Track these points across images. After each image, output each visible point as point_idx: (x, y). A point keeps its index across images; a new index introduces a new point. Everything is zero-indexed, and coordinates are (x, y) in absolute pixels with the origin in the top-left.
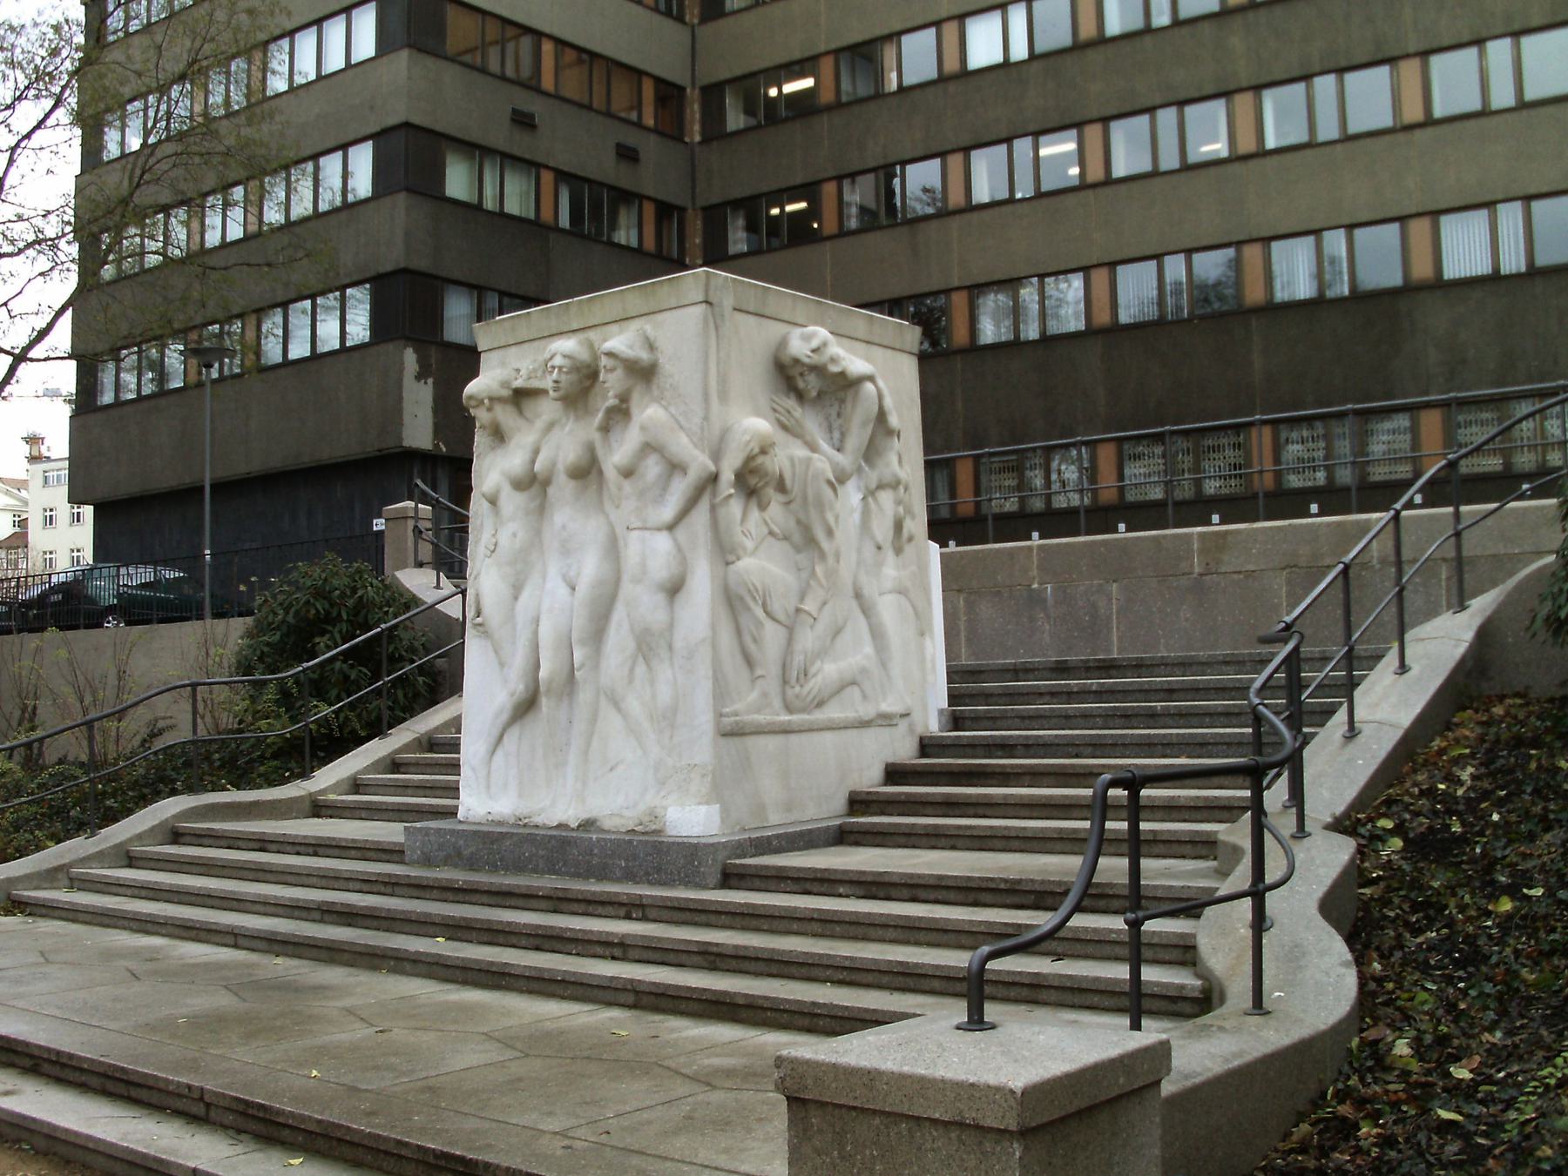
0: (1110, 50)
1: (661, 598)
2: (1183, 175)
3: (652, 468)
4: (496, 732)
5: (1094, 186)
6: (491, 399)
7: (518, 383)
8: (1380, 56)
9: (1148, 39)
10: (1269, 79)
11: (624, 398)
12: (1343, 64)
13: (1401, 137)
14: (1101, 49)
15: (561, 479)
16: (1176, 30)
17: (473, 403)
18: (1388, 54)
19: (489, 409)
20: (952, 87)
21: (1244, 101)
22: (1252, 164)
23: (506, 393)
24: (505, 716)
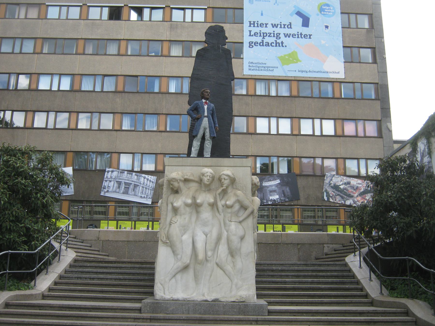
1: (240, 240)
3: (237, 207)
4: (174, 274)
5: (72, 129)
7: (186, 177)
9: (94, 93)
11: (227, 187)
12: (146, 112)
13: (159, 133)
14: (80, 93)
15: (206, 205)
16: (102, 93)
17: (173, 180)
18: (158, 113)
19: (178, 183)
20: (33, 93)
22: (118, 132)
23: (183, 179)
24: (179, 269)
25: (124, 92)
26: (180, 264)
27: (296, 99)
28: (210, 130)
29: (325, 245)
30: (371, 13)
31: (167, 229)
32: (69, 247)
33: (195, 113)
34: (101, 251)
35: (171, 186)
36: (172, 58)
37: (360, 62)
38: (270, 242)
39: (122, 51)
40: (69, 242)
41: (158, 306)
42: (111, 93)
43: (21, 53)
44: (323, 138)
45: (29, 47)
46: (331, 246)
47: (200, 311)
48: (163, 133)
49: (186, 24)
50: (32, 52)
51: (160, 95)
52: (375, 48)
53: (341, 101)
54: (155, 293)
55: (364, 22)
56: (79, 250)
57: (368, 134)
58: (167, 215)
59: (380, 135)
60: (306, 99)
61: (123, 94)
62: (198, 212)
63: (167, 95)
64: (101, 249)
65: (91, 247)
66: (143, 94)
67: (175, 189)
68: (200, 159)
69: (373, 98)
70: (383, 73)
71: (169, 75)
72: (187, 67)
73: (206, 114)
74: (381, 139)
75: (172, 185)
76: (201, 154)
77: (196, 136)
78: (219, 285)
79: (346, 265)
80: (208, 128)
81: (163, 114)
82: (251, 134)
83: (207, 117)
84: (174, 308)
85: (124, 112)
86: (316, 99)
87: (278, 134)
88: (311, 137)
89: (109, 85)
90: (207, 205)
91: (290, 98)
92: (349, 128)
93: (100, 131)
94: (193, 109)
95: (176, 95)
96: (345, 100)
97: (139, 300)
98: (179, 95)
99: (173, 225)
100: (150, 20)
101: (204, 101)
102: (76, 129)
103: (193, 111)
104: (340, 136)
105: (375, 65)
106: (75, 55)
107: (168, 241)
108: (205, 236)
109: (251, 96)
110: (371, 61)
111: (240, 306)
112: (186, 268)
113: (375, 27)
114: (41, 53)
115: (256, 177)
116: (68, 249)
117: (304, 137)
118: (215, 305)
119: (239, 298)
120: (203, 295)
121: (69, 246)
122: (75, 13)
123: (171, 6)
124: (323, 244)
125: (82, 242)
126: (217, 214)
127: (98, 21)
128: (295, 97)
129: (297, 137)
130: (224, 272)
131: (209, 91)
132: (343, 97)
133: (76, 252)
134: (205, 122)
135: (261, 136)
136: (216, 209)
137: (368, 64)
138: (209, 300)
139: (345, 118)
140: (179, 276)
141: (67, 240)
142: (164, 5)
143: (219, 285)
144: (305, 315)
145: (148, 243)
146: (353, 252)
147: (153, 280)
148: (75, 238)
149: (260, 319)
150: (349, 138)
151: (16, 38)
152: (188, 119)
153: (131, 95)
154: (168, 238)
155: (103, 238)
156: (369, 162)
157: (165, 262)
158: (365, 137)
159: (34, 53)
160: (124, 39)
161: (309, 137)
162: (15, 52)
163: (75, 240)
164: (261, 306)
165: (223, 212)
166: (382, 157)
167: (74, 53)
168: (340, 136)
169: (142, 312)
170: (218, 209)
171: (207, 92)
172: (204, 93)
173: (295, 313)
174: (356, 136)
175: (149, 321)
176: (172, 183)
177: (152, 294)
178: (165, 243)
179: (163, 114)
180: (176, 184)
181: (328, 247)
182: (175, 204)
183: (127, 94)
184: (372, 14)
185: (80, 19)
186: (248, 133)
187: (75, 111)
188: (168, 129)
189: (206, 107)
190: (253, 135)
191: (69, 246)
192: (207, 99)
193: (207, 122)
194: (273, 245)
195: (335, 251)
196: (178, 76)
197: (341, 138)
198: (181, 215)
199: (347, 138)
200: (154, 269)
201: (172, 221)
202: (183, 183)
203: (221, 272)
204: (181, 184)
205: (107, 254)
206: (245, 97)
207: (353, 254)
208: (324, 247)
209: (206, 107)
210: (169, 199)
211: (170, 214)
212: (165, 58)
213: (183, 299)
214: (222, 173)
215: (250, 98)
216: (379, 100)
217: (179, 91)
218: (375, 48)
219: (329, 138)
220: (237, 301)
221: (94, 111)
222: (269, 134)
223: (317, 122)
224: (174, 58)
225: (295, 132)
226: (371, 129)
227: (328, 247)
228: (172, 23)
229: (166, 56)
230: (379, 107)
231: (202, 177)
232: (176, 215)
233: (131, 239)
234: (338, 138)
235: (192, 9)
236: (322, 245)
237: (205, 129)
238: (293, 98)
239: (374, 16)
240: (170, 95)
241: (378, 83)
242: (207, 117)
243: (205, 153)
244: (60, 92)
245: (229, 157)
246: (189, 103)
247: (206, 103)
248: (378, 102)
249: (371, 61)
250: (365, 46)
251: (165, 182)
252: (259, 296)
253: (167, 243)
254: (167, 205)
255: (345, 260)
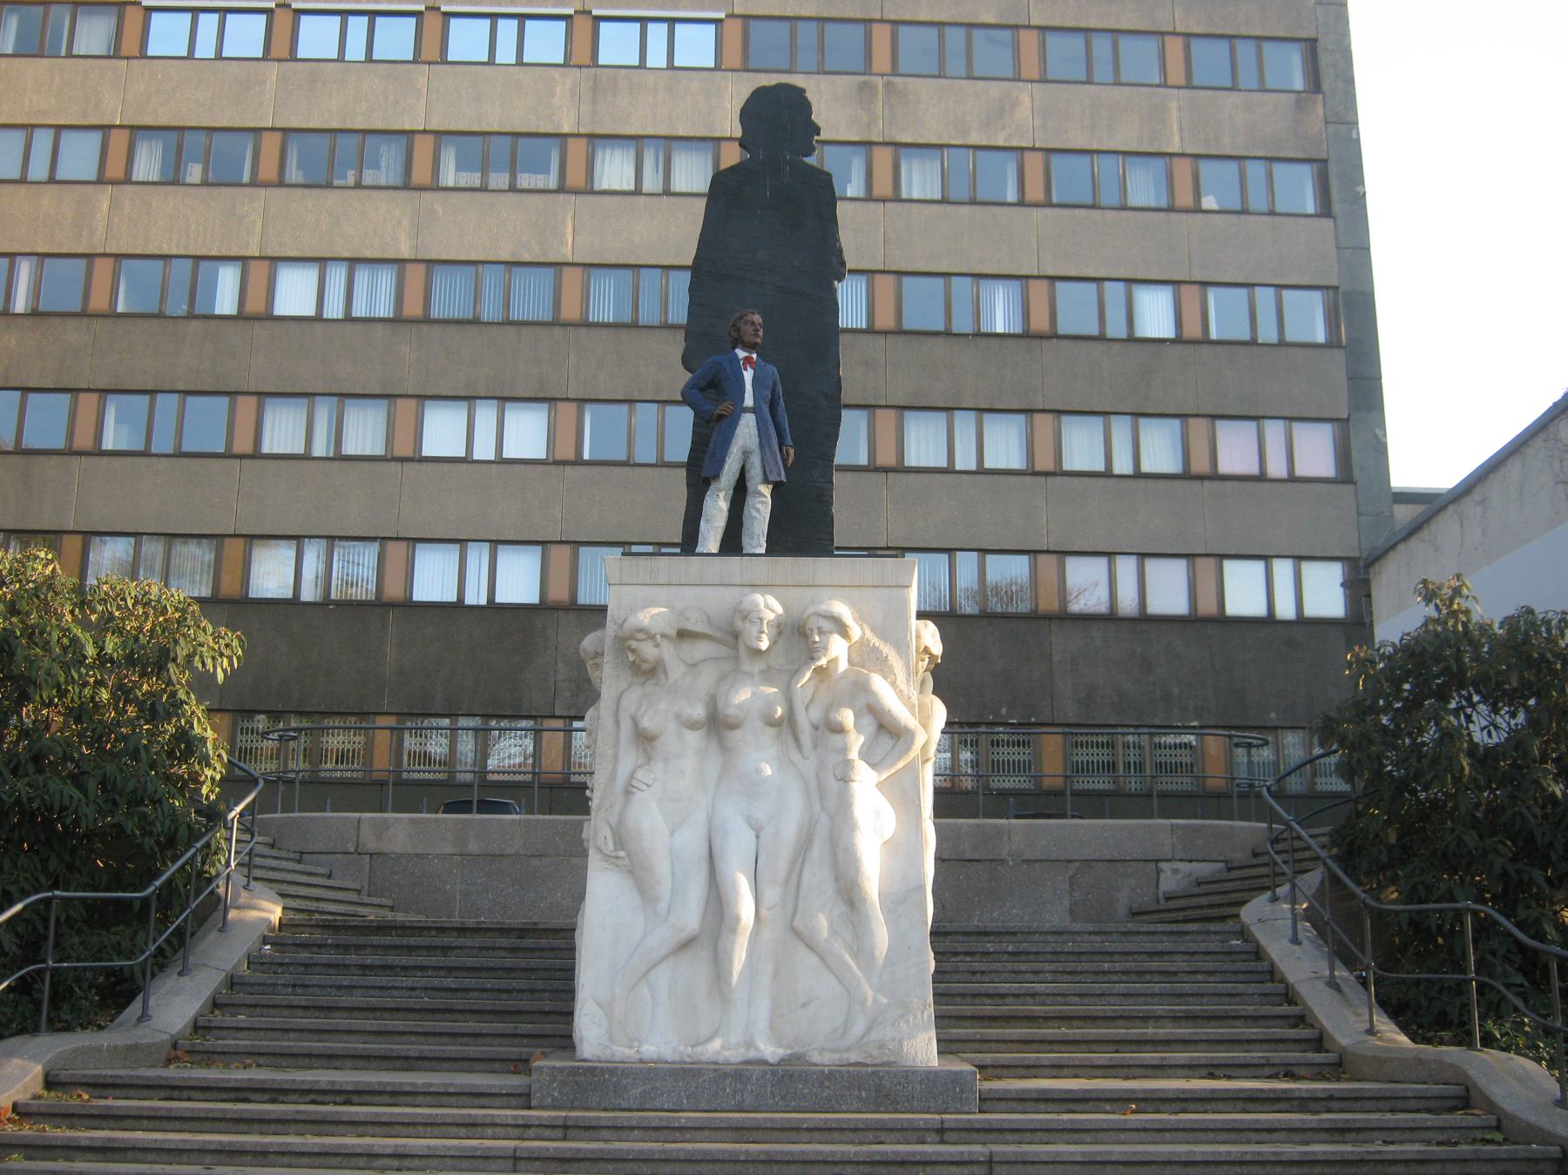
0: (278, 328)
2: (337, 463)
5: (241, 457)
6: (662, 636)
8: (542, 395)
9: (318, 326)
10: (435, 392)
12: (507, 394)
13: (553, 469)
14: (267, 324)
16: (349, 325)
17: (640, 636)
20: (97, 324)
21: (406, 407)
22: (407, 466)
23: (673, 632)
25: (427, 320)
26: (663, 937)
27: (1046, 344)
28: (763, 460)
29: (1163, 865)
30: (1312, 35)
31: (617, 809)
32: (255, 879)
33: (711, 400)
34: (365, 892)
35: (631, 658)
36: (598, 198)
37: (1272, 213)
38: (968, 856)
39: (421, 174)
40: (257, 860)
41: (601, 1081)
42: (379, 326)
43: (52, 180)
44: (1142, 483)
45: (80, 157)
46: (1185, 867)
47: (738, 1098)
48: (568, 468)
49: (650, 78)
50: (93, 177)
51: (557, 331)
52: (1325, 161)
53: (1206, 349)
54: (576, 1037)
55: (1289, 68)
56: (292, 890)
57: (1301, 470)
58: (616, 758)
59: (1345, 473)
60: (1080, 344)
61: (425, 328)
62: (725, 749)
63: (583, 330)
64: (366, 884)
65: (329, 877)
66: (495, 328)
67: (645, 666)
68: (735, 561)
69: (1320, 337)
70: (1356, 251)
71: (588, 261)
72: (677, 234)
73: (749, 401)
74: (1351, 487)
75: (633, 651)
76: (732, 543)
77: (717, 477)
78: (803, 1005)
79: (1244, 933)
80: (758, 451)
81: (567, 399)
82: (886, 470)
83: (753, 410)
84: (648, 1087)
85: (429, 393)
86: (1116, 347)
87: (981, 471)
88: (1101, 481)
89: (375, 295)
90: (761, 724)
91: (1022, 342)
92: (1236, 450)
93: (343, 464)
94: (703, 384)
95: (612, 331)
96: (1219, 348)
97: (521, 1065)
98: (624, 333)
99: (638, 795)
100: (520, 62)
101: (741, 354)
102: (257, 455)
103: (702, 390)
104: (1201, 478)
105: (1327, 223)
106: (248, 190)
107: (622, 854)
108: (751, 836)
109: (886, 333)
110: (1310, 209)
111: (881, 1078)
112: (686, 945)
113: (1325, 87)
114: (127, 180)
115: (930, 624)
116: (253, 883)
117: (1076, 480)
118: (791, 1076)
119: (876, 1052)
120: (749, 1044)
121: (257, 873)
122: (246, 36)
123: (595, 12)
124: (1157, 861)
125: (299, 862)
126: (795, 755)
127: (332, 65)
128: (1041, 337)
129: (1050, 479)
130: (822, 958)
131: (757, 318)
132: (1214, 335)
133: (282, 895)
134: (747, 431)
135: (920, 477)
136: (790, 739)
137: (1302, 221)
138: (771, 1060)
139: (1220, 412)
140: (662, 976)
141: (250, 853)
142: (568, 6)
143: (803, 1005)
144: (1108, 1107)
145: (535, 862)
146: (1268, 888)
147: (569, 993)
148: (272, 846)
149: (953, 1125)
150: (1235, 484)
151: (33, 126)
152: (682, 420)
153: (452, 330)
154: (620, 842)
155: (371, 844)
156: (1308, 568)
157: (611, 926)
158: (1292, 479)
159: (100, 181)
160: (424, 132)
161: (1092, 480)
162: (31, 176)
163: (274, 852)
164: (955, 1078)
165: (815, 747)
166: (1356, 554)
167: (246, 178)
168: (1201, 478)
169: (534, 1103)
170: (796, 739)
171: (753, 323)
172: (740, 324)
173: (1075, 1100)
174: (1261, 477)
175: (559, 1133)
176: (634, 644)
177: (565, 1041)
178: (607, 858)
179: (567, 399)
180: (648, 651)
181: (1175, 871)
182: (646, 723)
183: (437, 329)
184: (1315, 40)
185: (267, 56)
186: (872, 468)
187: (252, 389)
188: (586, 456)
189: (748, 375)
190: (891, 475)
191: (257, 873)
192: (750, 347)
193: (754, 431)
194: (980, 866)
195: (1199, 884)
196: (621, 262)
197: (1207, 483)
198: (666, 760)
199: (1228, 484)
200: (572, 949)
201: (635, 783)
202: (671, 646)
203: (811, 959)
204: (667, 651)
205: (390, 903)
206: (863, 339)
207: (1268, 894)
208: (1159, 871)
209: (748, 375)
210: (624, 703)
211: (628, 759)
212: (573, 197)
213: (677, 1058)
214: (811, 610)
215: (881, 340)
216: (1339, 346)
217: (628, 319)
218: (1325, 161)
219: (1162, 484)
220: (868, 1061)
221: (321, 390)
222: (949, 470)
223: (1121, 429)
224: (606, 198)
225: (1044, 463)
226: (1315, 453)
227: (1175, 871)
228: (599, 70)
229: (576, 192)
230: (1342, 375)
231: (739, 624)
232: (649, 758)
233: (473, 847)
234: (1197, 485)
235: (672, 22)
236: (1153, 865)
237: (746, 454)
238: (1036, 342)
239: (1320, 45)
240: (594, 332)
241: (1336, 288)
242: (753, 410)
243: (745, 540)
244: (195, 323)
245: (829, 554)
246: (687, 362)
247: (748, 360)
248: (1339, 356)
249: (1310, 209)
250: (1291, 155)
251: (608, 642)
252: (946, 1046)
253: (617, 857)
254: (617, 723)
255: (1237, 916)
